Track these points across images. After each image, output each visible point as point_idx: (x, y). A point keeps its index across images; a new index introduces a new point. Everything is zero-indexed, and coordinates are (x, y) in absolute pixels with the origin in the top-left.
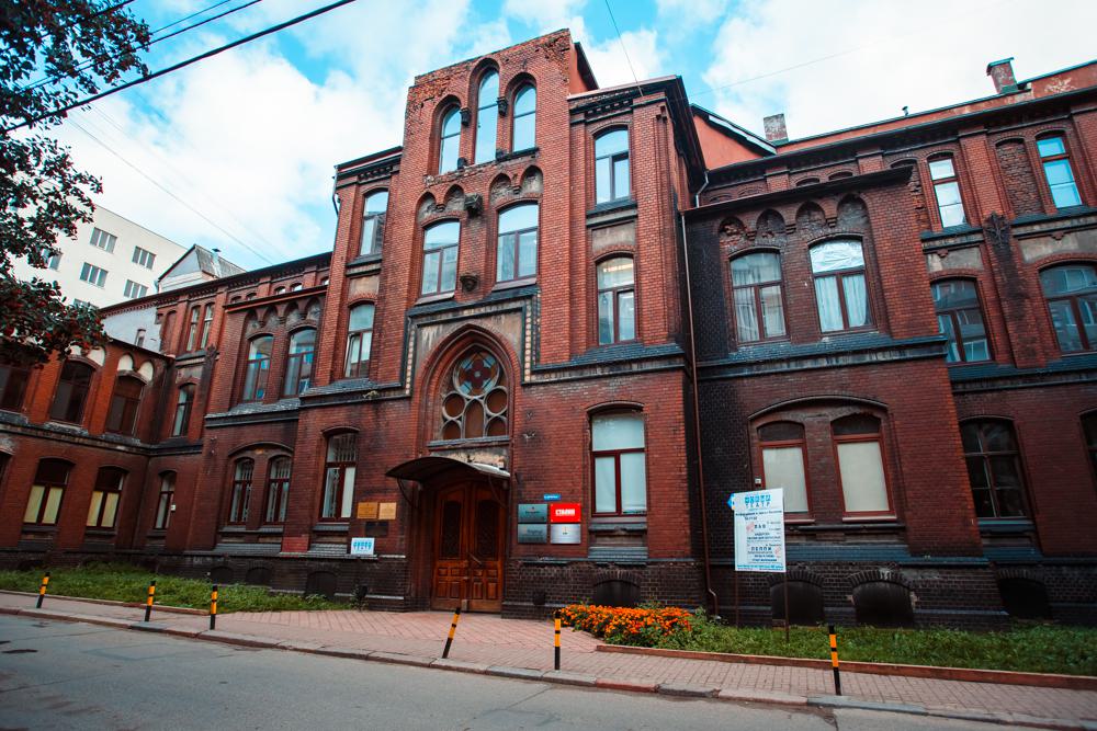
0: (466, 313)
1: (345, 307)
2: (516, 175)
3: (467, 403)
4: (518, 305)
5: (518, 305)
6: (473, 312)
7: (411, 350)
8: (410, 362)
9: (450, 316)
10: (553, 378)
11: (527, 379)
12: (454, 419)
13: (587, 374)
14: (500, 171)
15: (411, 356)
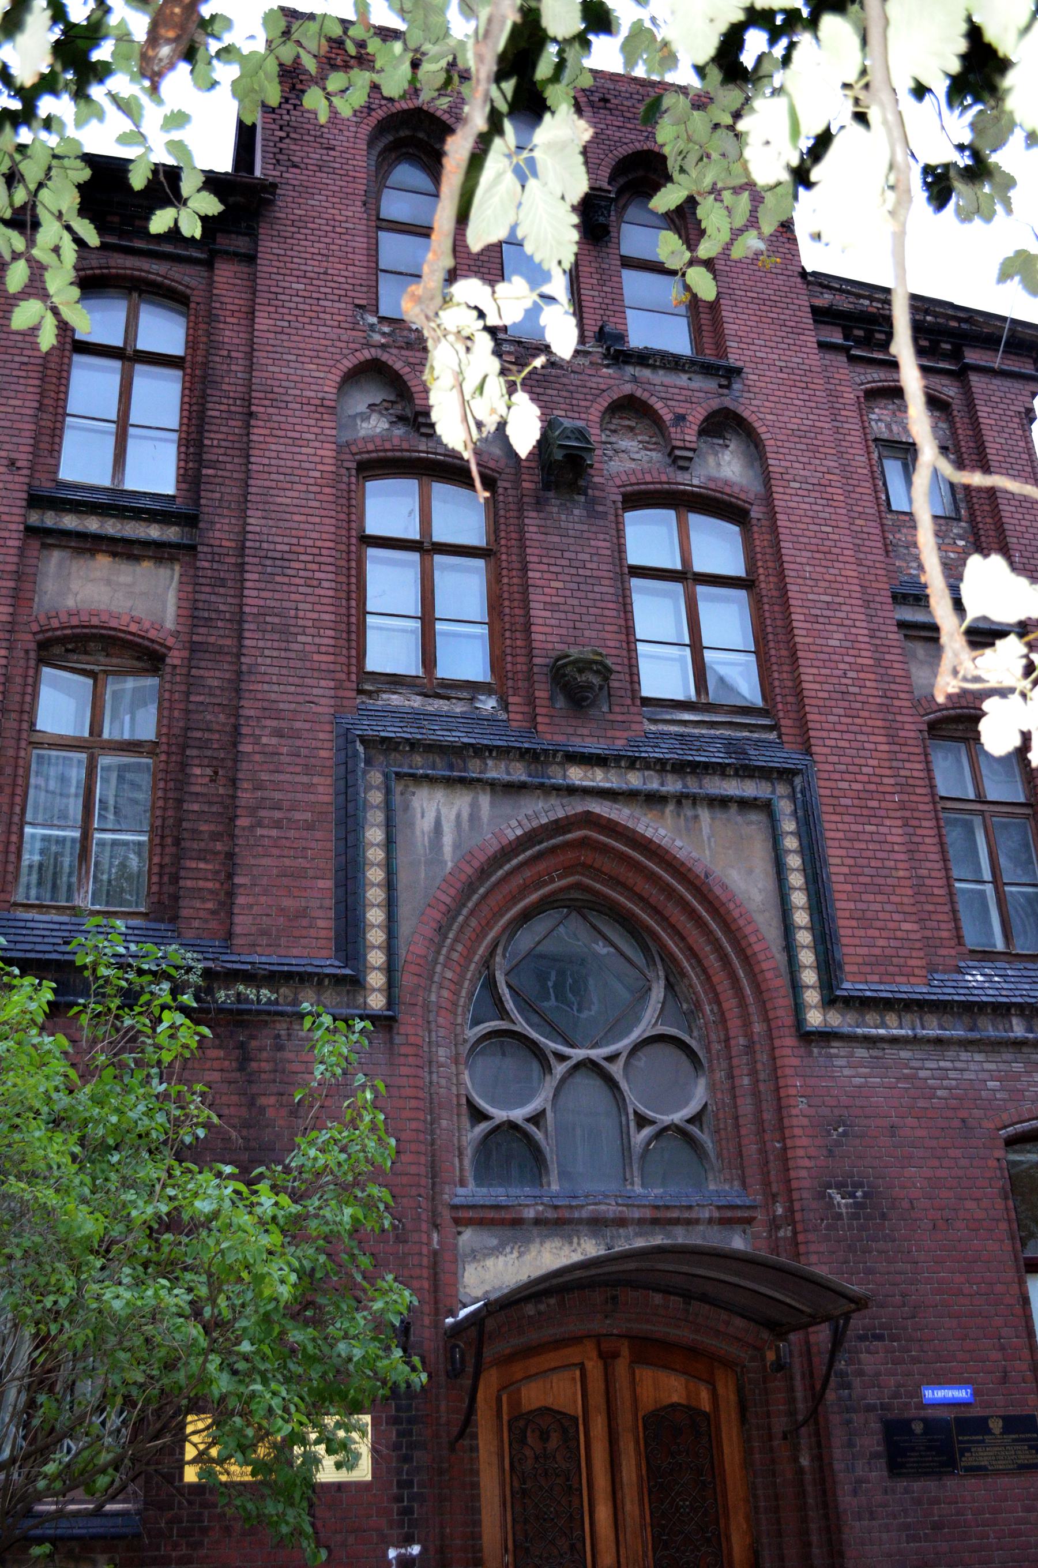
0: (576, 775)
1: (27, 640)
2: (680, 418)
3: (560, 1069)
4: (750, 789)
5: (750, 789)
6: (599, 778)
7: (376, 854)
8: (375, 895)
9: (519, 773)
10: (893, 1027)
11: (815, 1018)
12: (518, 1114)
13: (990, 1030)
14: (628, 388)
15: (375, 875)
